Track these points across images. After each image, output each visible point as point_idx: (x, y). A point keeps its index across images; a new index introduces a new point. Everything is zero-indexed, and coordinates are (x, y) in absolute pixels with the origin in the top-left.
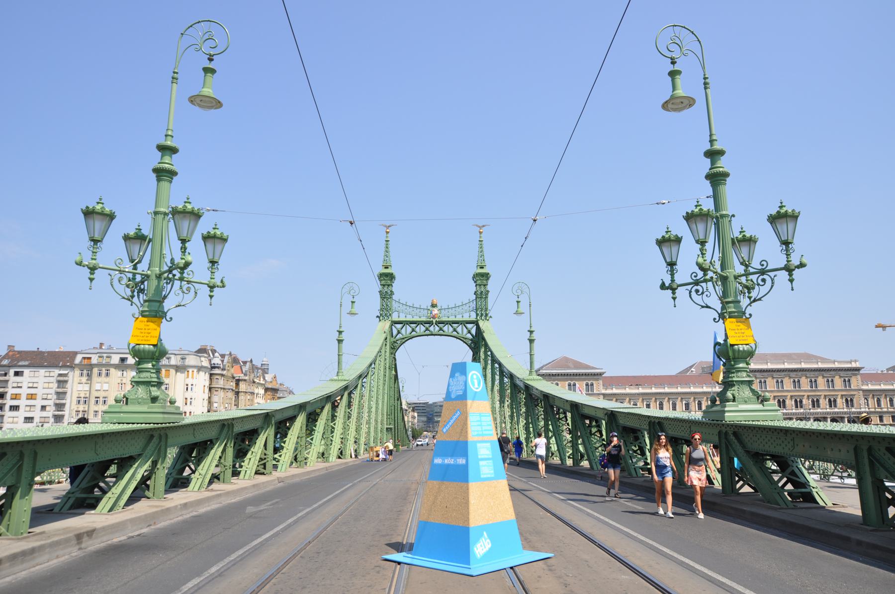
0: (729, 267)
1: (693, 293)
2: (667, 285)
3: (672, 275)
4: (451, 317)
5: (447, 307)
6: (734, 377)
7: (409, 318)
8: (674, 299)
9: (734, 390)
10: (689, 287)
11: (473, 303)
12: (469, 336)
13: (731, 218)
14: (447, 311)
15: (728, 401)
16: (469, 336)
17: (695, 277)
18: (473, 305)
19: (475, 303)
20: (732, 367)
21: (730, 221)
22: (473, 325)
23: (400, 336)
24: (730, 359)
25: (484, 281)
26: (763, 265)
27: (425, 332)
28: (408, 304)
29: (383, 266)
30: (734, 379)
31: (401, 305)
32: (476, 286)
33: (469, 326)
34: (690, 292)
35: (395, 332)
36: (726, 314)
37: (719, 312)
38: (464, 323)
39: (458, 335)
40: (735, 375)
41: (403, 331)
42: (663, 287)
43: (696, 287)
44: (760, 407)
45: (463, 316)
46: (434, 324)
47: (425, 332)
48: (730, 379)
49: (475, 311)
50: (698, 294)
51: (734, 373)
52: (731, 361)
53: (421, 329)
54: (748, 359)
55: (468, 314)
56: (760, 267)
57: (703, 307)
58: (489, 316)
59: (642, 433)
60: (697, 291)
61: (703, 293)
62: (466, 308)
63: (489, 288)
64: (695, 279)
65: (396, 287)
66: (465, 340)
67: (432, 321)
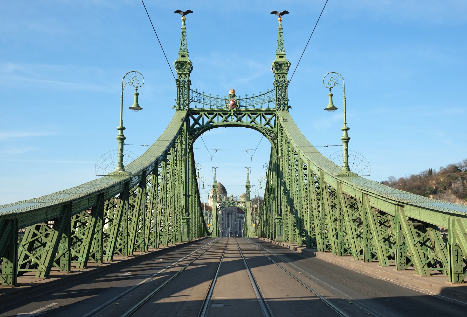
7: (207, 107)
14: (245, 101)
18: (273, 95)
19: (274, 92)
23: (197, 126)
29: (179, 54)
31: (198, 96)
33: (268, 117)
35: (192, 122)
41: (201, 121)
46: (232, 114)
53: (218, 120)
62: (265, 98)
65: (193, 77)
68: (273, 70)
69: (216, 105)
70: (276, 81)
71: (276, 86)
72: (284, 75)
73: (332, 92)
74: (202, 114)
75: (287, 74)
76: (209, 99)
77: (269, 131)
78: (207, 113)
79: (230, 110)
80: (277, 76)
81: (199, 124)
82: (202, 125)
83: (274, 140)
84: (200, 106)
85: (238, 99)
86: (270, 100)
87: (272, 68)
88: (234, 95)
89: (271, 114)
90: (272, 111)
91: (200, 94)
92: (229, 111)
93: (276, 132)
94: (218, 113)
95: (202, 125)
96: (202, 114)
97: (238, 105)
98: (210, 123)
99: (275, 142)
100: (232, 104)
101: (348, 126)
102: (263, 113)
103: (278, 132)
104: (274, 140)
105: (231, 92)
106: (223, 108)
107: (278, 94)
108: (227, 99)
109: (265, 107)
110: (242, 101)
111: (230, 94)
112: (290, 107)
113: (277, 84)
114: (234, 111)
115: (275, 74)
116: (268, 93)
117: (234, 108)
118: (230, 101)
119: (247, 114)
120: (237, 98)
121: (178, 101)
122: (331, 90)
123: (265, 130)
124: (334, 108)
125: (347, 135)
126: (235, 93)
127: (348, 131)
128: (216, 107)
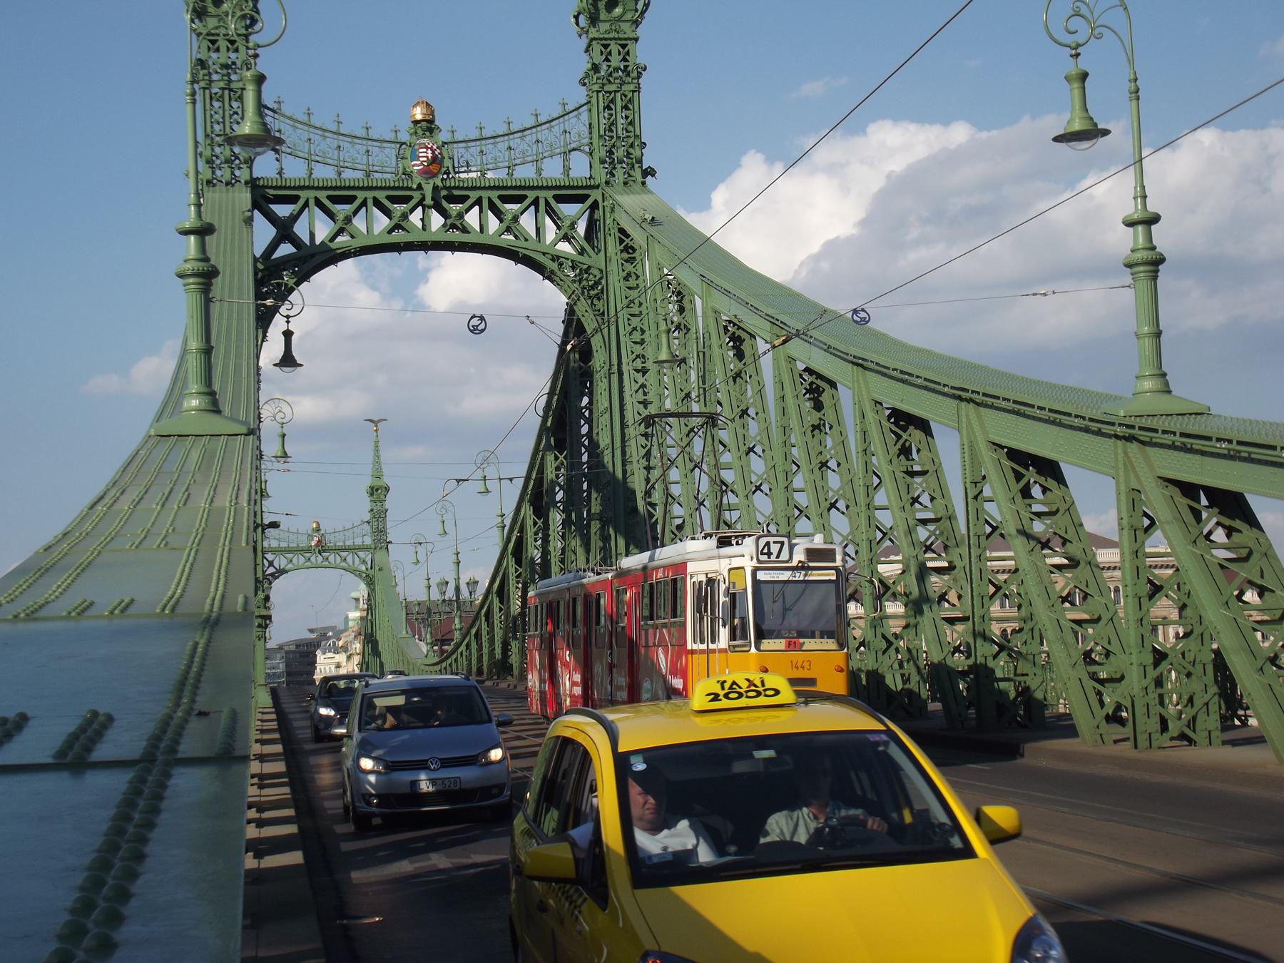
4: (490, 175)
5: (475, 134)
7: (324, 173)
11: (580, 114)
12: (564, 247)
14: (474, 150)
18: (578, 127)
22: (579, 206)
27: (390, 232)
28: (316, 121)
33: (568, 210)
39: (522, 243)
41: (301, 229)
45: (539, 171)
46: (429, 201)
47: (390, 232)
55: (558, 161)
63: (640, 54)
67: (420, 187)
68: (577, 24)
69: (359, 167)
70: (596, 68)
71: (596, 87)
72: (624, 46)
73: (1083, 64)
74: (307, 201)
75: (636, 40)
76: (332, 142)
77: (573, 268)
78: (329, 197)
79: (420, 183)
80: (597, 47)
81: (295, 241)
82: (308, 244)
83: (595, 301)
84: (295, 170)
85: (446, 143)
86: (574, 145)
87: (576, 17)
88: (428, 126)
89: (580, 199)
90: (582, 187)
91: (297, 121)
92: (415, 186)
93: (601, 271)
94: (370, 194)
95: (308, 244)
96: (307, 201)
97: (447, 163)
98: (339, 239)
99: (599, 311)
100: (425, 159)
101: (1152, 207)
102: (549, 194)
103: (613, 267)
104: (595, 301)
105: (418, 113)
106: (389, 179)
107: (603, 121)
108: (403, 141)
109: (552, 171)
110: (463, 151)
111: (416, 122)
112: (649, 172)
113: (597, 79)
114: (436, 188)
115: (592, 40)
116: (564, 115)
117: (434, 175)
118: (417, 147)
119: (485, 203)
120: (443, 136)
121: (209, 148)
122: (1078, 55)
123: (561, 264)
124: (1093, 133)
125: (1148, 245)
126: (433, 116)
127: (1153, 227)
128: (360, 175)
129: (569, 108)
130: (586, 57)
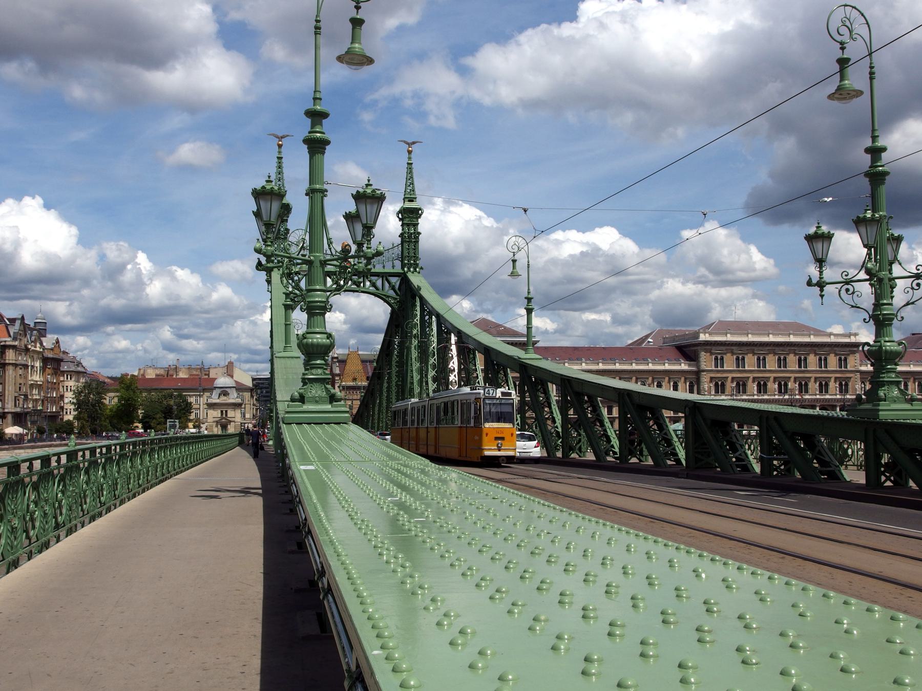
0: (884, 269)
1: (843, 291)
2: (814, 281)
3: (821, 272)
6: (885, 377)
8: (822, 296)
9: (885, 390)
10: (839, 286)
11: (398, 248)
13: (888, 220)
15: (881, 400)
16: (391, 293)
17: (846, 275)
19: (400, 248)
20: (883, 367)
21: (887, 222)
22: (398, 278)
24: (881, 359)
25: (415, 220)
26: (918, 270)
30: (885, 379)
32: (402, 225)
34: (840, 291)
36: (880, 316)
37: (871, 313)
38: (385, 276)
39: (378, 292)
40: (885, 375)
42: (809, 283)
43: (846, 286)
44: (908, 406)
48: (881, 379)
49: (400, 259)
50: (848, 293)
51: (884, 373)
52: (882, 362)
54: (897, 360)
56: (916, 272)
57: (853, 306)
58: (420, 266)
59: (731, 428)
60: (847, 290)
61: (853, 293)
63: (420, 228)
64: (845, 277)
66: (387, 299)
129: (395, 245)
130: (401, 228)
